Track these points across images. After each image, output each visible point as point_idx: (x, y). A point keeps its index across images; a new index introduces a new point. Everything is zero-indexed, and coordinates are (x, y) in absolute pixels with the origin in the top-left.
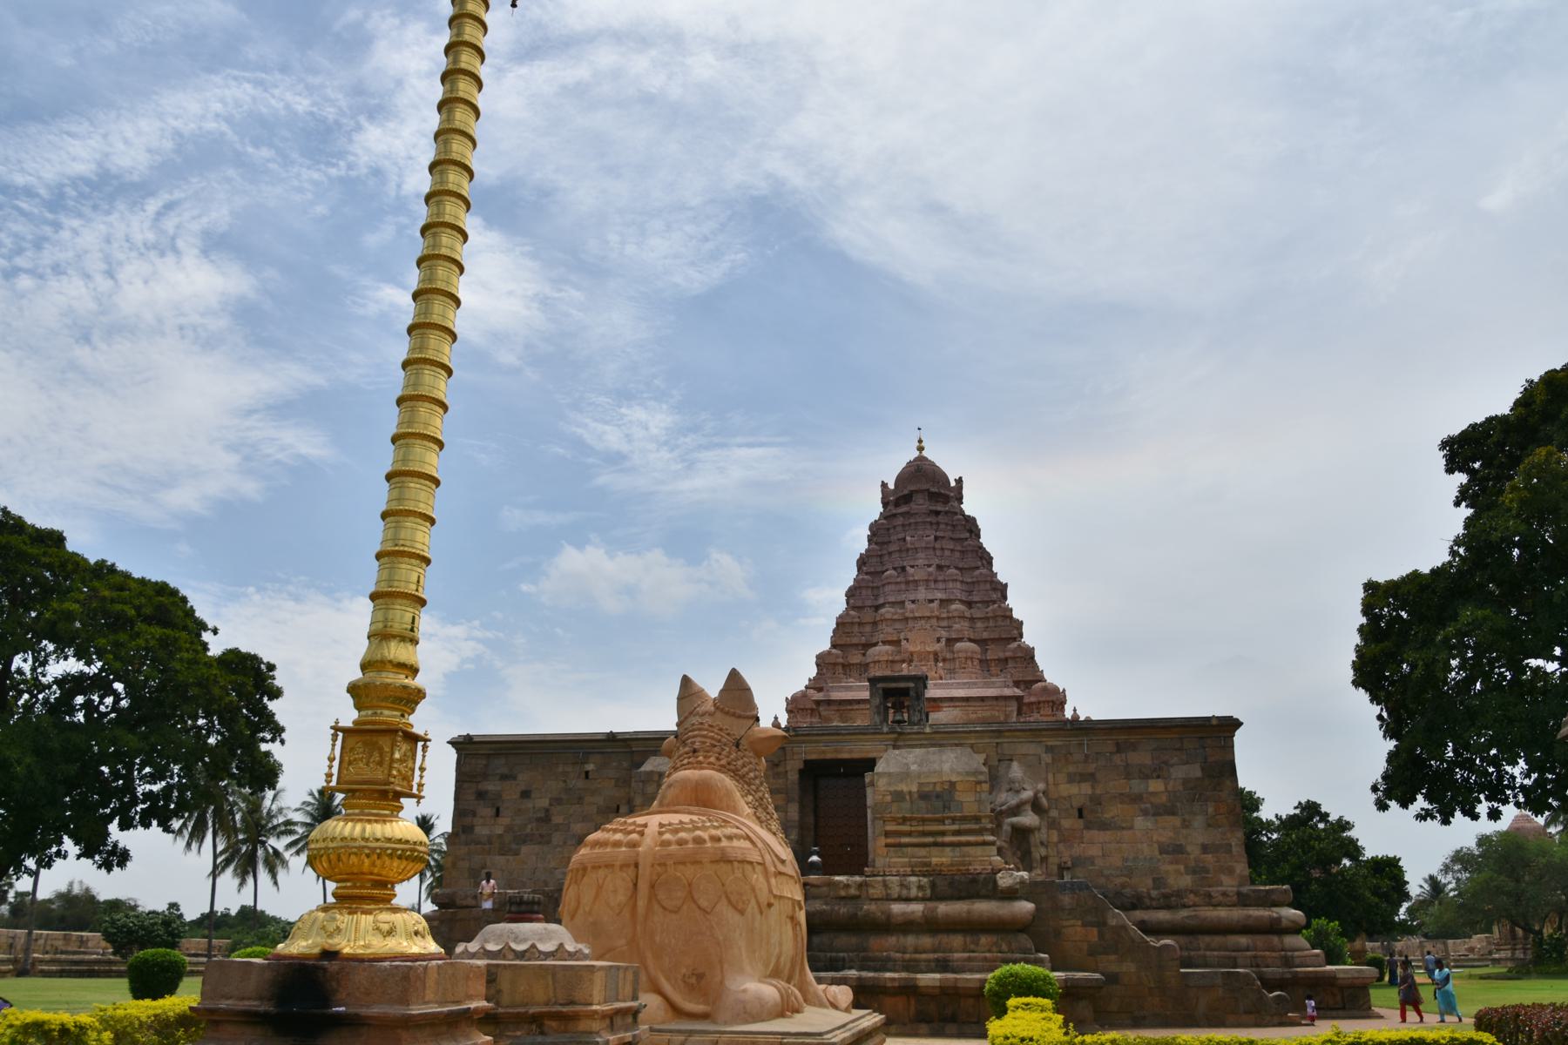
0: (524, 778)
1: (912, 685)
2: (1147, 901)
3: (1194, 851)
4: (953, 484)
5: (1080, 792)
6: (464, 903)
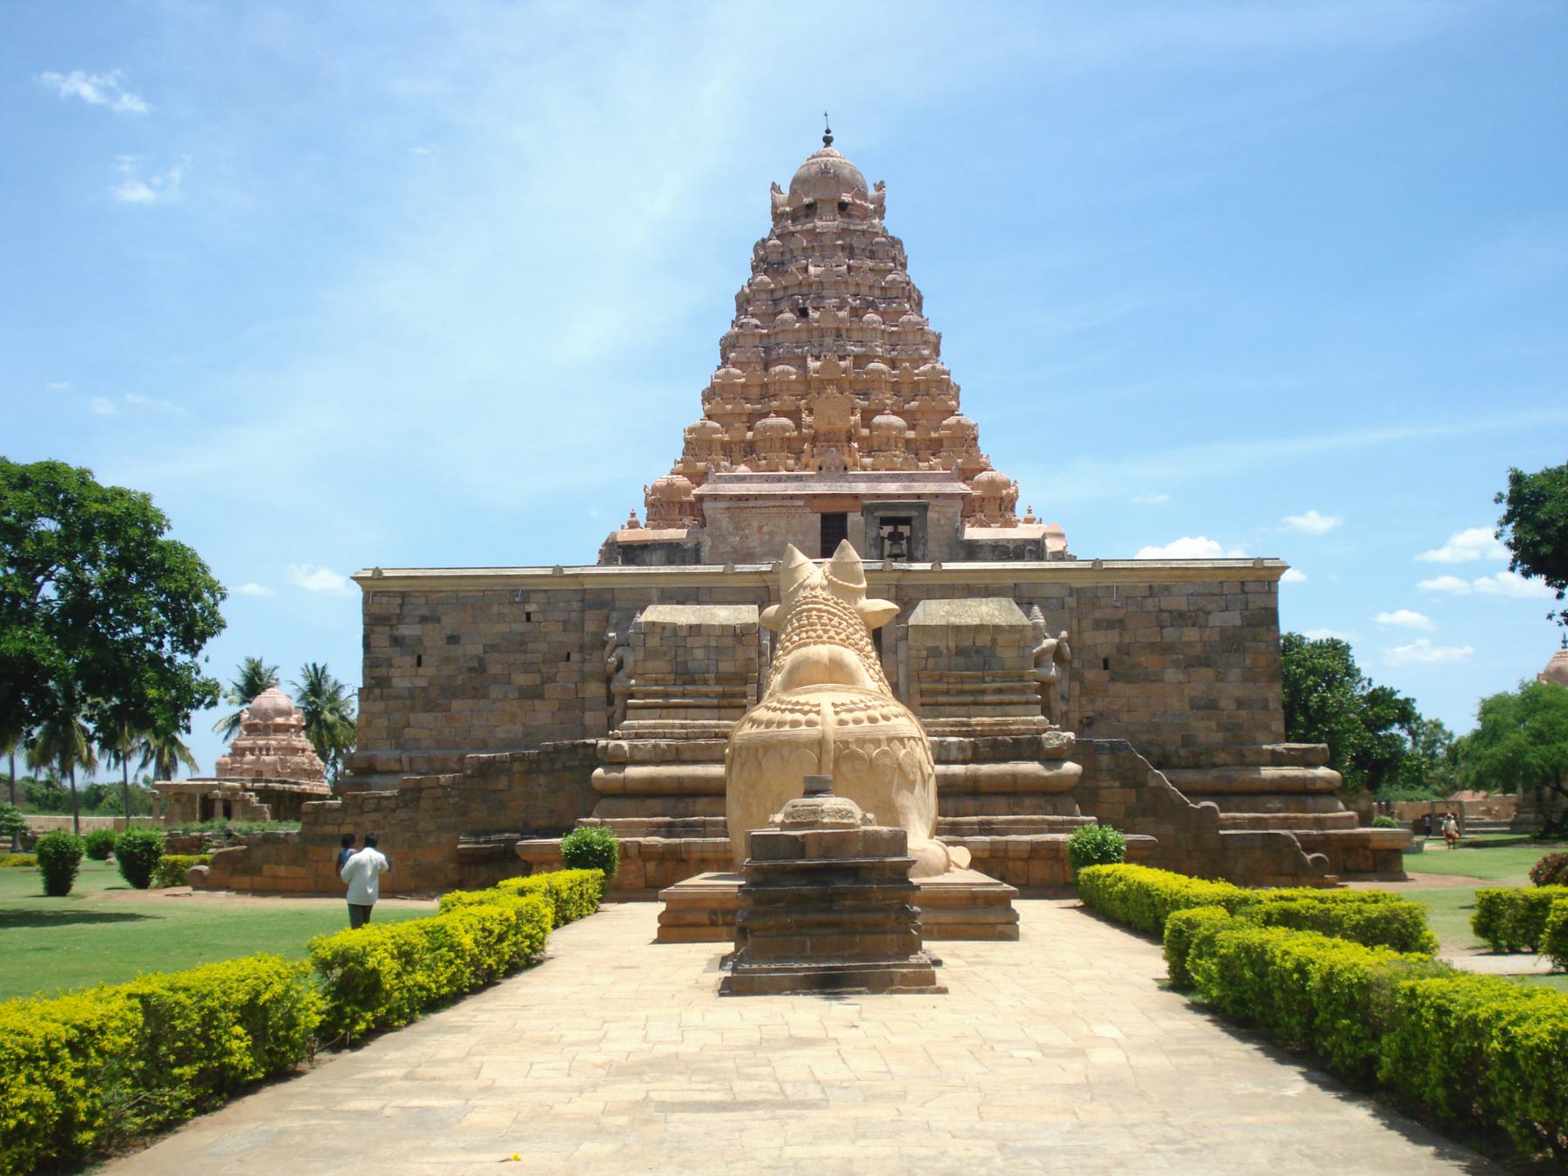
0: (449, 622)
1: (914, 514)
2: (1175, 760)
3: (1226, 704)
4: (872, 192)
5: (1105, 641)
6: (387, 768)
